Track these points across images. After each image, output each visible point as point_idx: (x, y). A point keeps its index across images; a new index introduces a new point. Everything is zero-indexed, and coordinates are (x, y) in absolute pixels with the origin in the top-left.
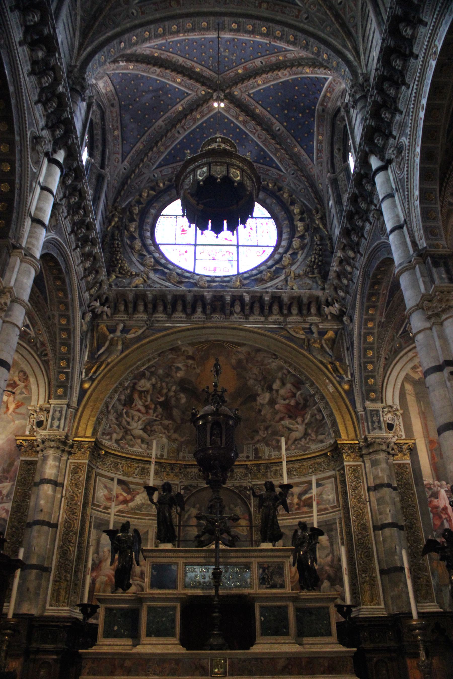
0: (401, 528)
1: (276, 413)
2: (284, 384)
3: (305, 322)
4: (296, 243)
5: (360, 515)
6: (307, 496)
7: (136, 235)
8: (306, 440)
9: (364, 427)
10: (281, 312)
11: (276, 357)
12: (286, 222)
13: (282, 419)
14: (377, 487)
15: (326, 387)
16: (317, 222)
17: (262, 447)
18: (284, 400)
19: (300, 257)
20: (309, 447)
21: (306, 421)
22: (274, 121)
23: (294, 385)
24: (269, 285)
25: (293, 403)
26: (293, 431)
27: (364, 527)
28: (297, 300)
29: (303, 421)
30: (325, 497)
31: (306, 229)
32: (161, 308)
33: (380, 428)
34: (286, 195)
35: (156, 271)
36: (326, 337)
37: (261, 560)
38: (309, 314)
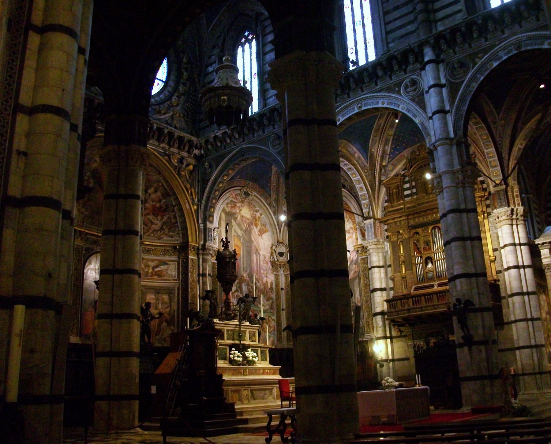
2: (156, 191)
3: (179, 153)
6: (158, 269)
8: (161, 232)
9: (202, 236)
10: (169, 144)
11: (160, 173)
13: (148, 214)
15: (185, 204)
16: (195, 76)
18: (153, 202)
20: (163, 238)
21: (164, 220)
23: (162, 195)
24: (163, 117)
25: (158, 205)
26: (154, 224)
28: (181, 139)
29: (162, 219)
30: (169, 272)
33: (211, 240)
37: (250, 330)
38: (183, 150)
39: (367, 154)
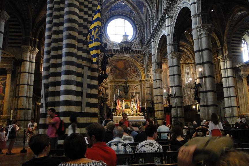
0: (150, 94)
1: (131, 72)
2: (133, 67)
4: (137, 36)
5: (144, 92)
7: (104, 32)
10: (133, 53)
12: (135, 29)
13: (132, 73)
14: (147, 88)
17: (128, 78)
19: (137, 39)
22: (134, 4)
27: (145, 94)
31: (139, 32)
32: (110, 52)
34: (136, 22)
35: (108, 42)
36: (141, 58)
38: (138, 54)
39: (188, 42)
